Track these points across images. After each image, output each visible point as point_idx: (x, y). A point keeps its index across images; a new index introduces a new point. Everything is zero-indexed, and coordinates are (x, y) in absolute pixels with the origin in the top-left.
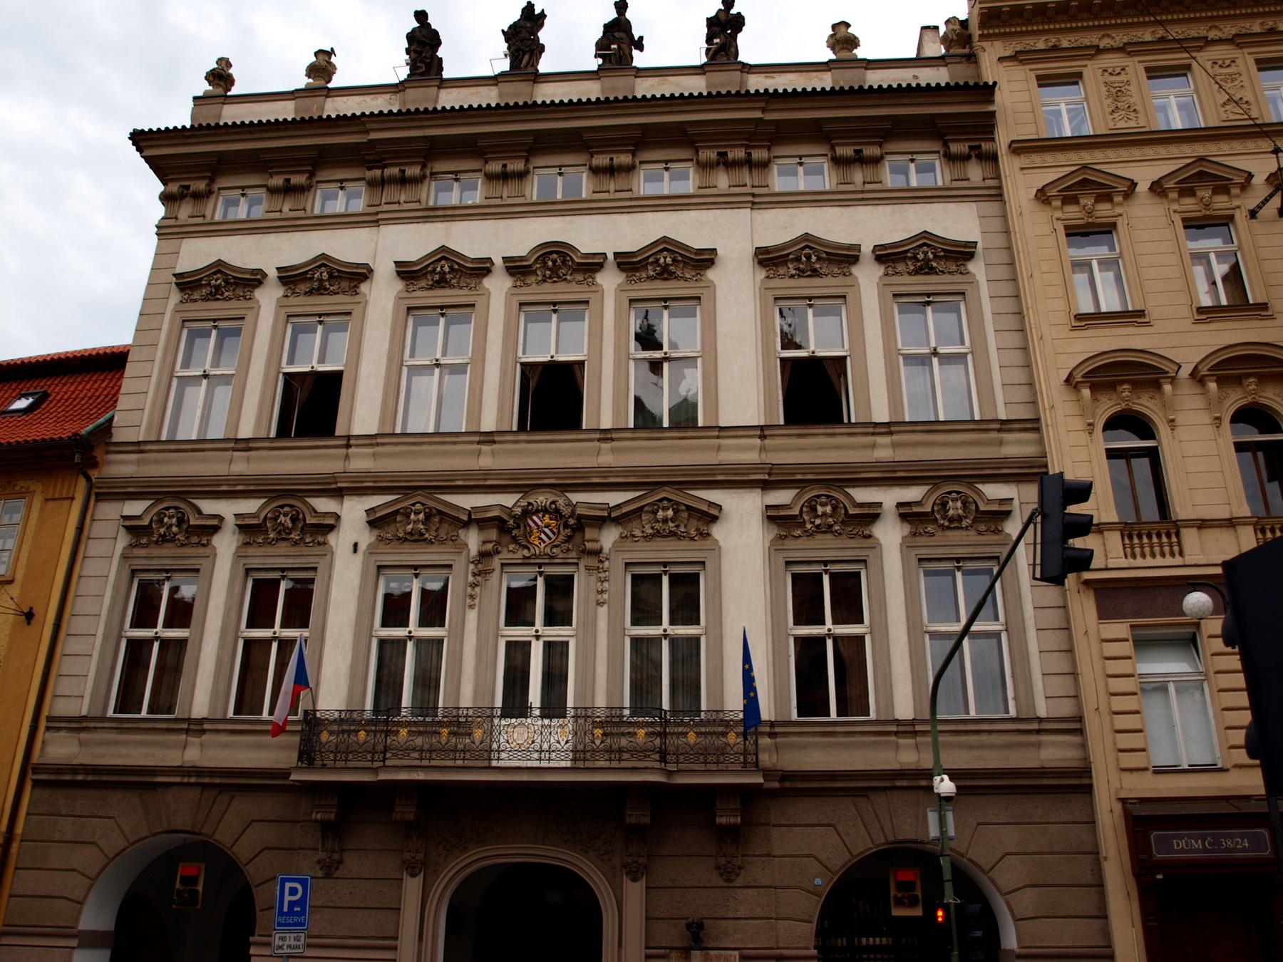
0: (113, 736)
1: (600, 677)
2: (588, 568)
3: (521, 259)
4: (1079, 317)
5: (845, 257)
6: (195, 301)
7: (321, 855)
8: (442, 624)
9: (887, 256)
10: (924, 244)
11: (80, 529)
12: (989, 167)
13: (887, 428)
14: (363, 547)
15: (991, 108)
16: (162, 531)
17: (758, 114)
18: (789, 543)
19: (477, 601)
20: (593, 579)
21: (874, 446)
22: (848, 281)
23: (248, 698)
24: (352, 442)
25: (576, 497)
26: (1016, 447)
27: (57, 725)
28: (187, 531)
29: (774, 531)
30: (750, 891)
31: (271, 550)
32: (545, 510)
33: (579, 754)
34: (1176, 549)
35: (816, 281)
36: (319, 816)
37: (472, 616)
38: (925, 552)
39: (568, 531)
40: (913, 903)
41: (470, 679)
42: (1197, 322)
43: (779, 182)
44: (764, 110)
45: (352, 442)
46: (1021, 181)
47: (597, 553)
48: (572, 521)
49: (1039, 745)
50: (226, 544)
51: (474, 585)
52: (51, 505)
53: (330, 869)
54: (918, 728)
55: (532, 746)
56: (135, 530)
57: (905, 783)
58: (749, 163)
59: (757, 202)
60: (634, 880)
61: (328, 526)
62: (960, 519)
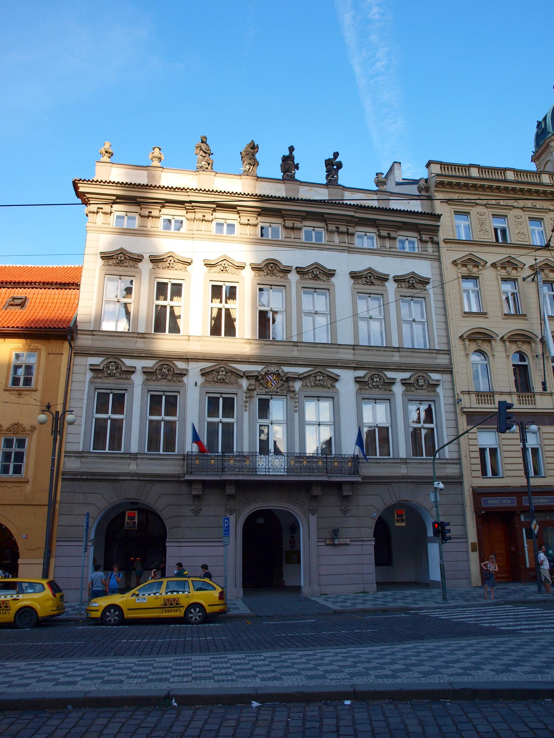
0: (97, 460)
2: (291, 398)
3: (258, 264)
4: (465, 313)
5: (383, 279)
6: (111, 265)
7: (193, 508)
8: (233, 417)
9: (398, 280)
10: (412, 277)
11: (69, 369)
12: (435, 246)
13: (399, 349)
14: (199, 384)
15: (438, 224)
16: (109, 372)
17: (352, 214)
18: (363, 391)
19: (248, 408)
20: (292, 402)
21: (393, 356)
23: (153, 443)
24: (191, 338)
26: (442, 360)
27: (69, 455)
28: (120, 373)
29: (358, 386)
30: (352, 518)
31: (158, 383)
32: (274, 374)
33: (289, 470)
34: (492, 401)
35: (372, 287)
36: (195, 493)
37: (246, 414)
38: (410, 398)
40: (402, 521)
42: (504, 319)
43: (357, 242)
44: (355, 212)
45: (191, 338)
46: (449, 255)
47: (294, 392)
49: (446, 468)
50: (138, 379)
51: (246, 402)
52: (51, 356)
53: (196, 513)
54: (408, 461)
56: (94, 369)
57: (403, 481)
58: (348, 233)
59: (351, 250)
60: (313, 515)
61: (183, 374)
62: (423, 386)
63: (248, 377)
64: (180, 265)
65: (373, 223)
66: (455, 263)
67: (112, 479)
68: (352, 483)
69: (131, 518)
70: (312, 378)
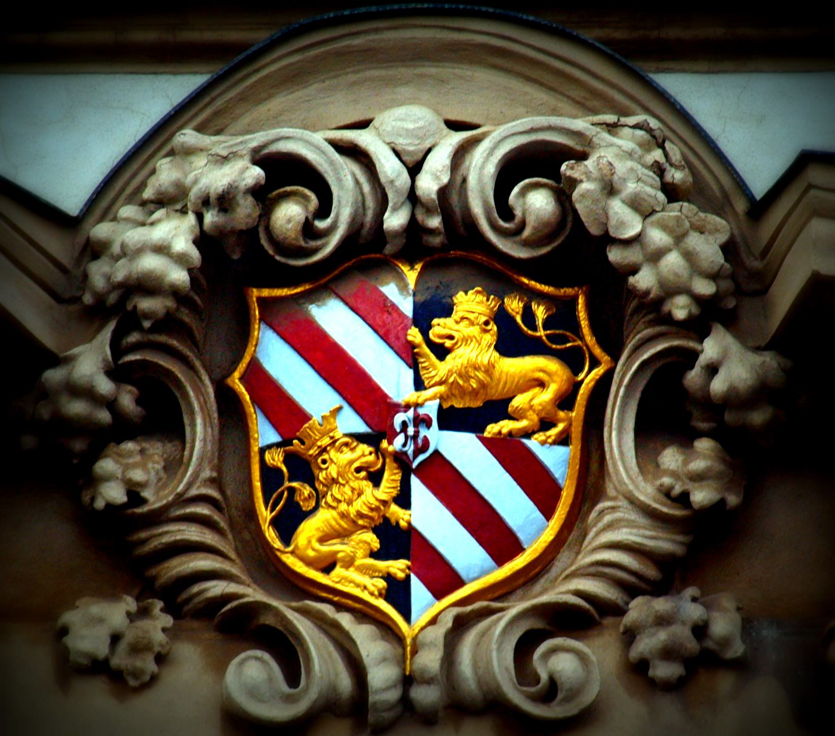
32: (450, 247)
39: (692, 465)
48: (729, 364)
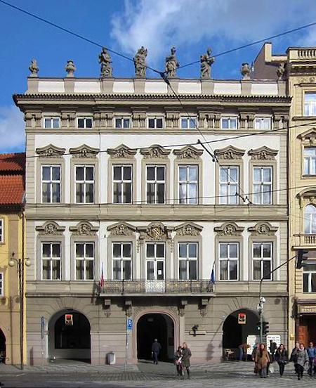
1: (172, 271)
15: (290, 105)
21: (243, 211)
22: (241, 161)
25: (165, 224)
41: (138, 272)
50: (67, 234)
53: (108, 316)
55: (155, 287)
56: (39, 230)
63: (139, 231)
64: (91, 155)
65: (236, 110)
66: (299, 137)
67: (56, 296)
68: (208, 298)
69: (69, 319)
70: (183, 229)
